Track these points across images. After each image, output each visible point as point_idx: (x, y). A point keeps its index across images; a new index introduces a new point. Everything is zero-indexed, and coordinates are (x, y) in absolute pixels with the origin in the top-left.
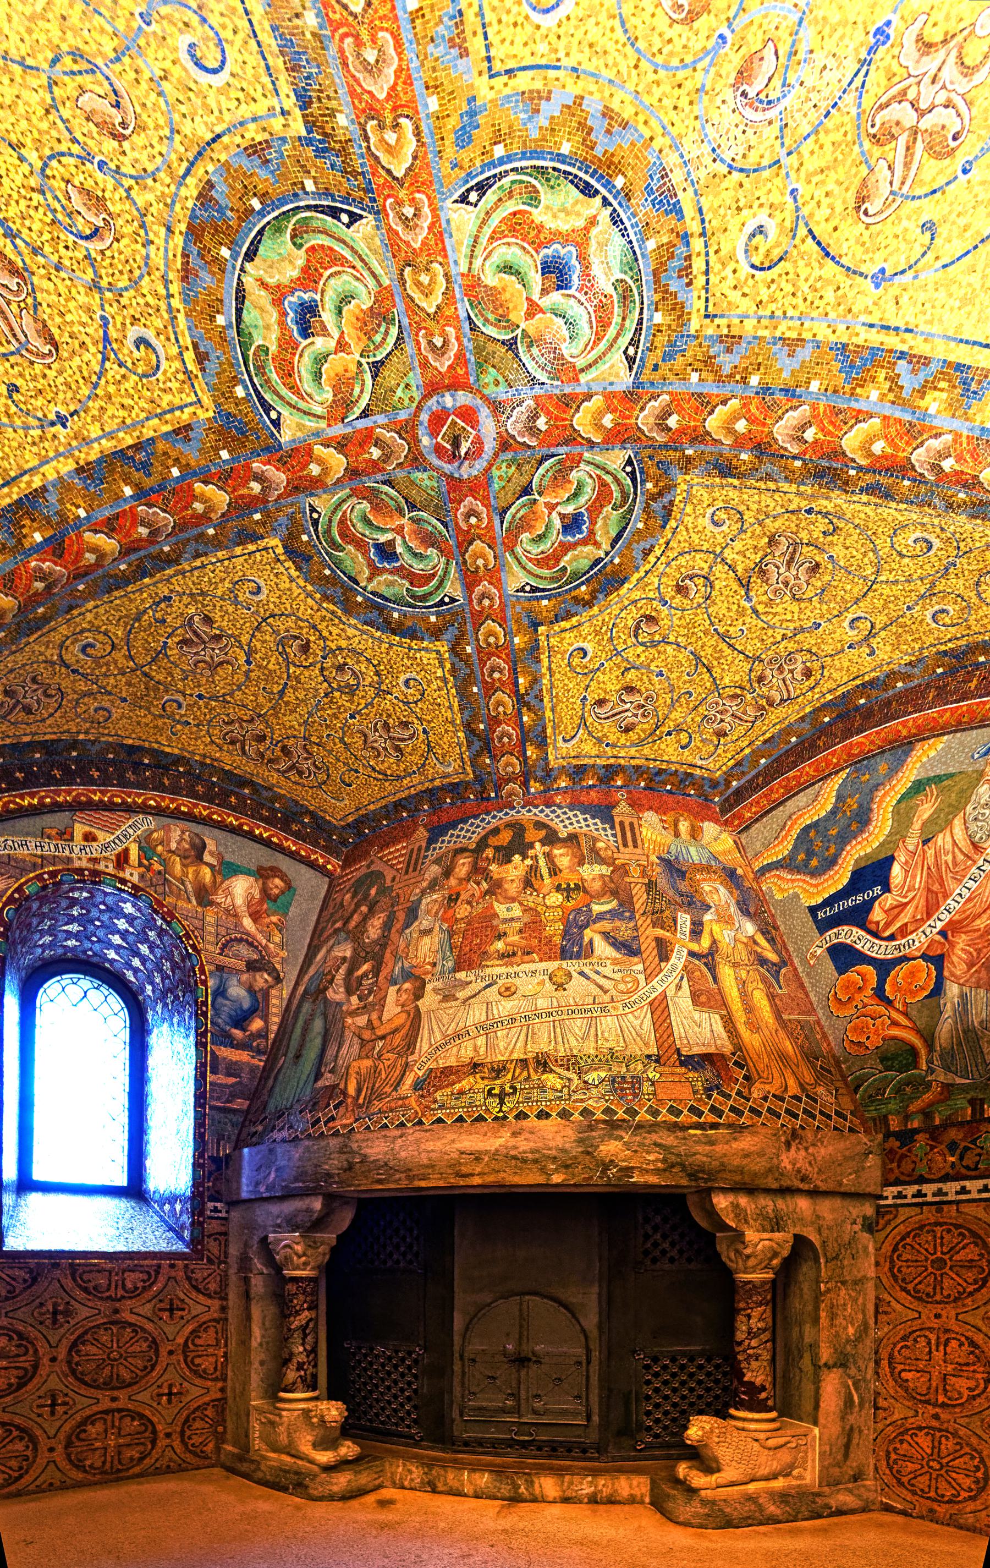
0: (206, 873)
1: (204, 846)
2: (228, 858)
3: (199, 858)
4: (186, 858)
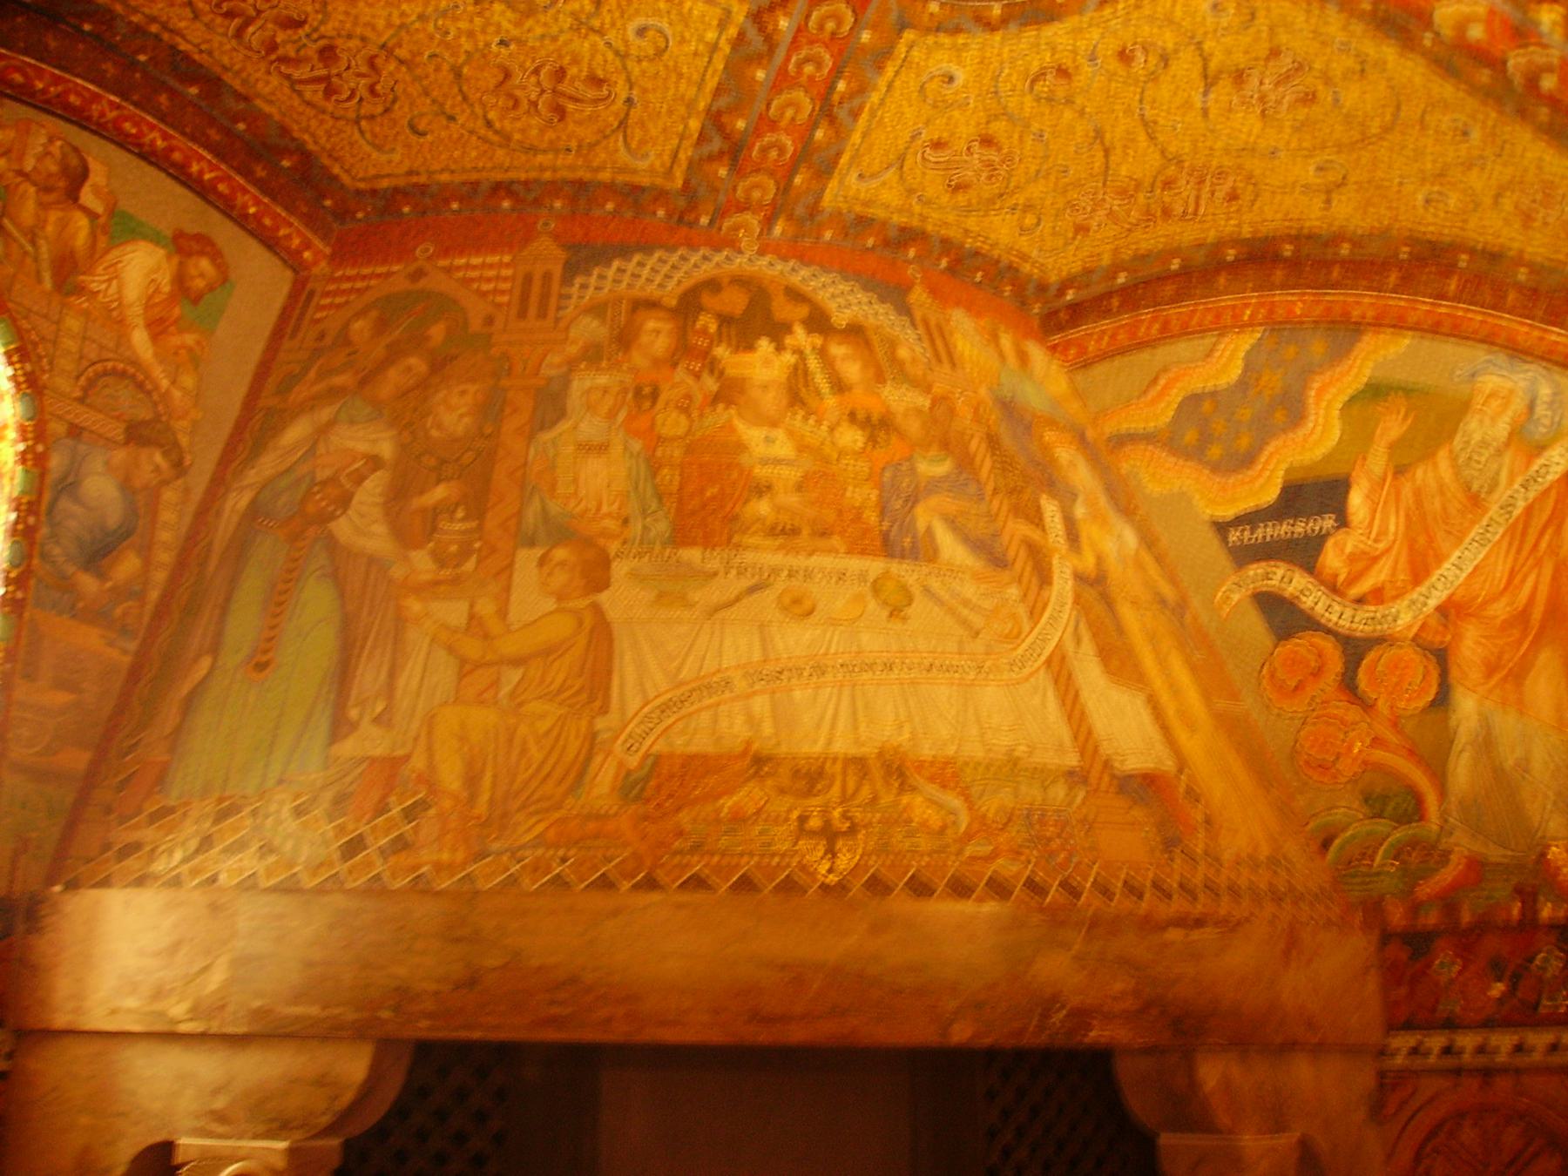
1: (84, 174)
3: (73, 195)
4: (48, 190)
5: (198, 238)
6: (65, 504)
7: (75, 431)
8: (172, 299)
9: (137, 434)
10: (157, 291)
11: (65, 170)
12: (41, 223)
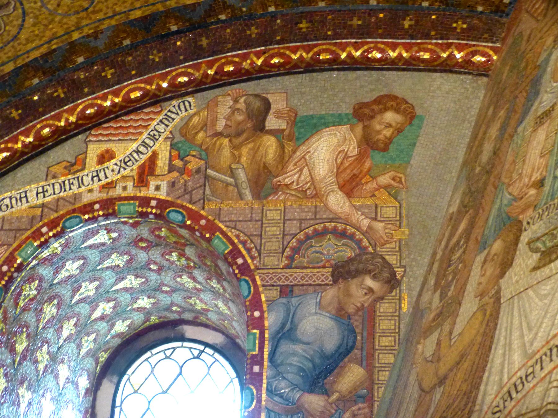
0: (270, 144)
2: (303, 112)
3: (260, 128)
5: (378, 101)
6: (285, 347)
7: (286, 291)
8: (361, 157)
9: (342, 272)
10: (346, 157)
11: (250, 115)
12: (237, 159)
